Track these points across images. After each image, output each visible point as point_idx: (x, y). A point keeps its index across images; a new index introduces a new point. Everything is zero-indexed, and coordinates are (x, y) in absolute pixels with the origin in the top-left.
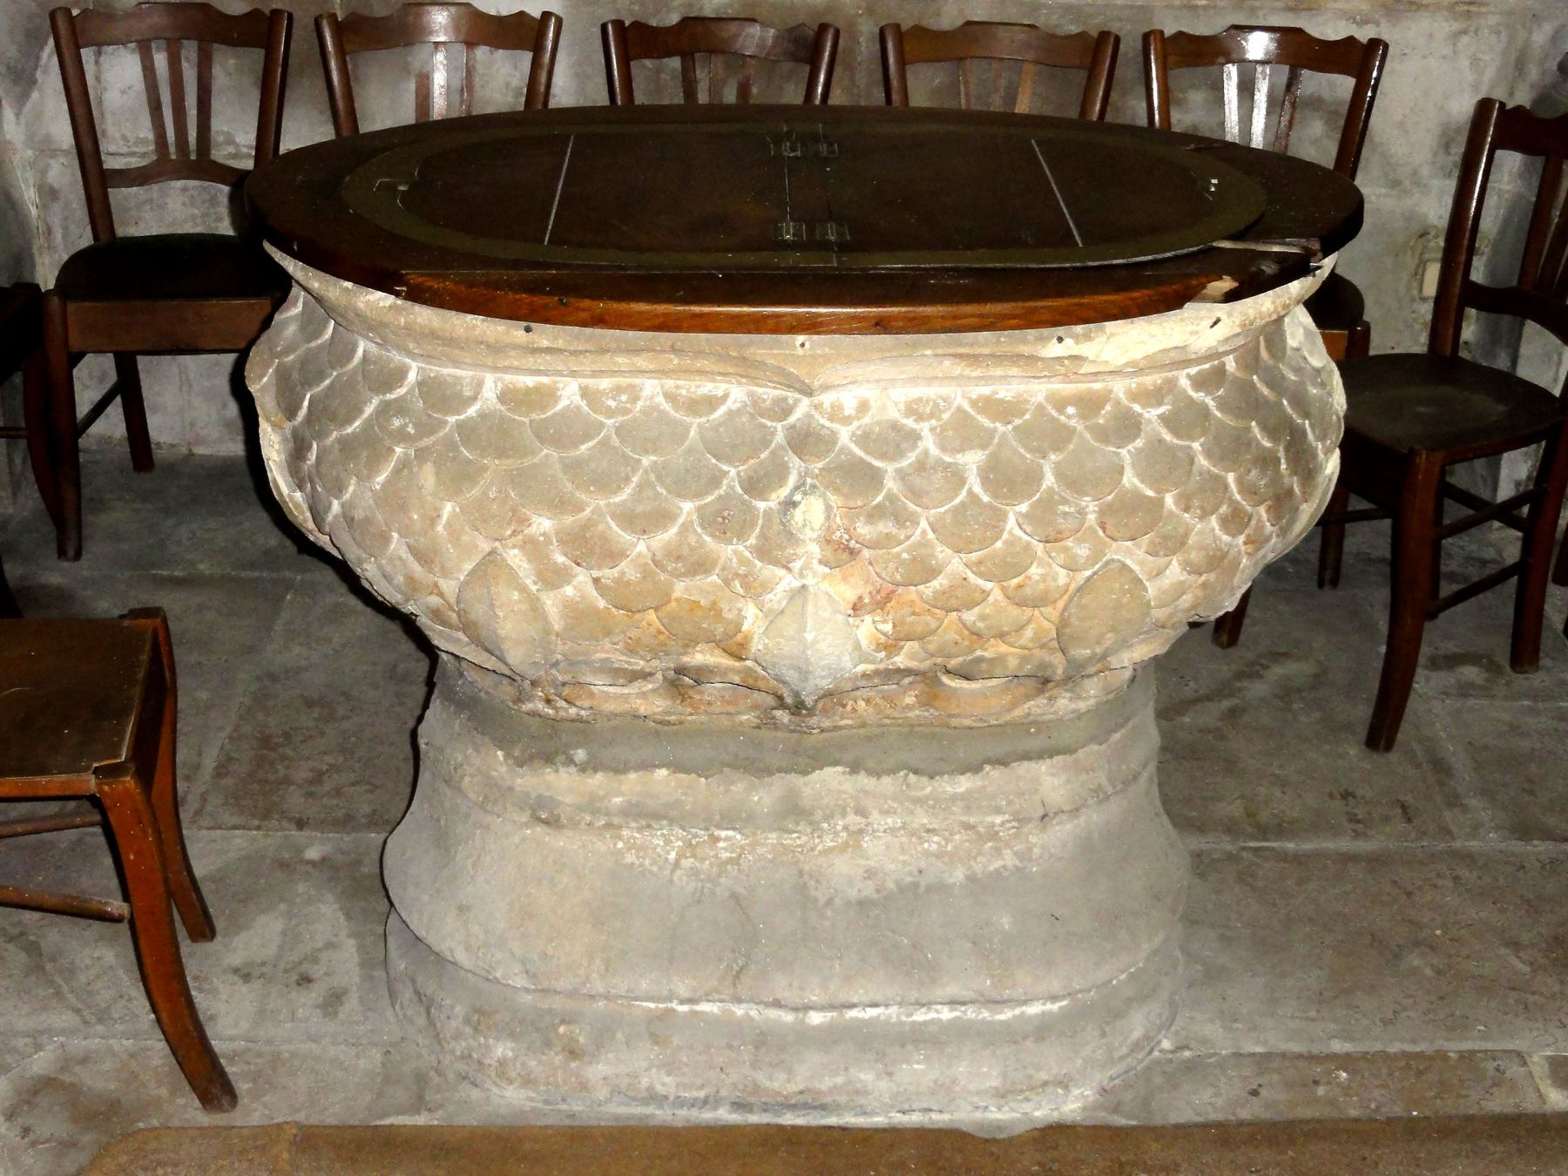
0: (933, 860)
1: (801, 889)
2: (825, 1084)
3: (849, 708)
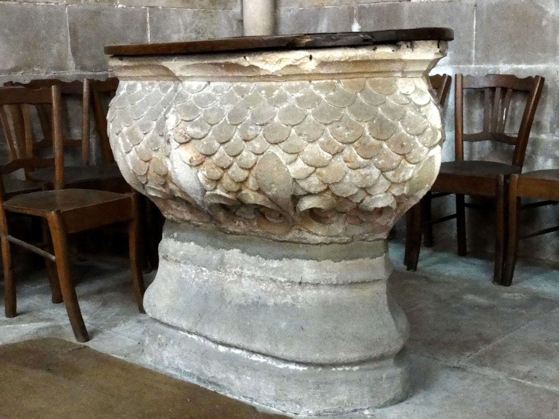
0: (263, 294)
1: (222, 295)
2: (221, 376)
3: (237, 224)
